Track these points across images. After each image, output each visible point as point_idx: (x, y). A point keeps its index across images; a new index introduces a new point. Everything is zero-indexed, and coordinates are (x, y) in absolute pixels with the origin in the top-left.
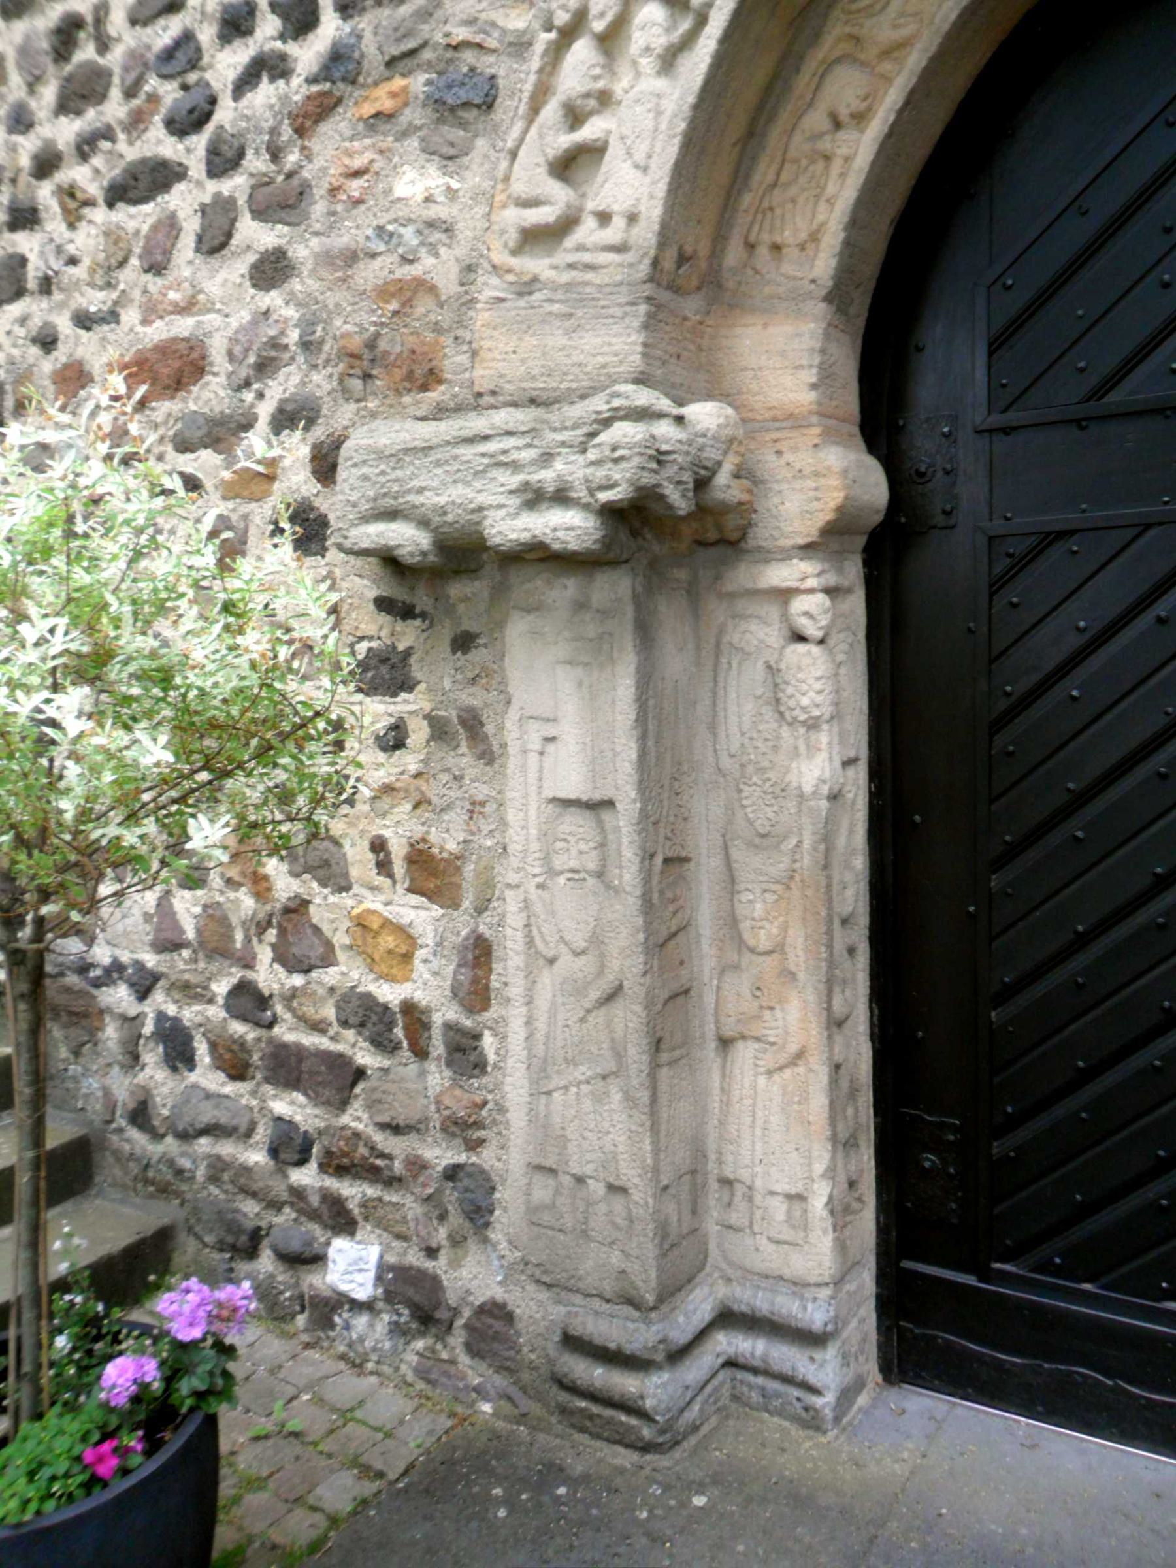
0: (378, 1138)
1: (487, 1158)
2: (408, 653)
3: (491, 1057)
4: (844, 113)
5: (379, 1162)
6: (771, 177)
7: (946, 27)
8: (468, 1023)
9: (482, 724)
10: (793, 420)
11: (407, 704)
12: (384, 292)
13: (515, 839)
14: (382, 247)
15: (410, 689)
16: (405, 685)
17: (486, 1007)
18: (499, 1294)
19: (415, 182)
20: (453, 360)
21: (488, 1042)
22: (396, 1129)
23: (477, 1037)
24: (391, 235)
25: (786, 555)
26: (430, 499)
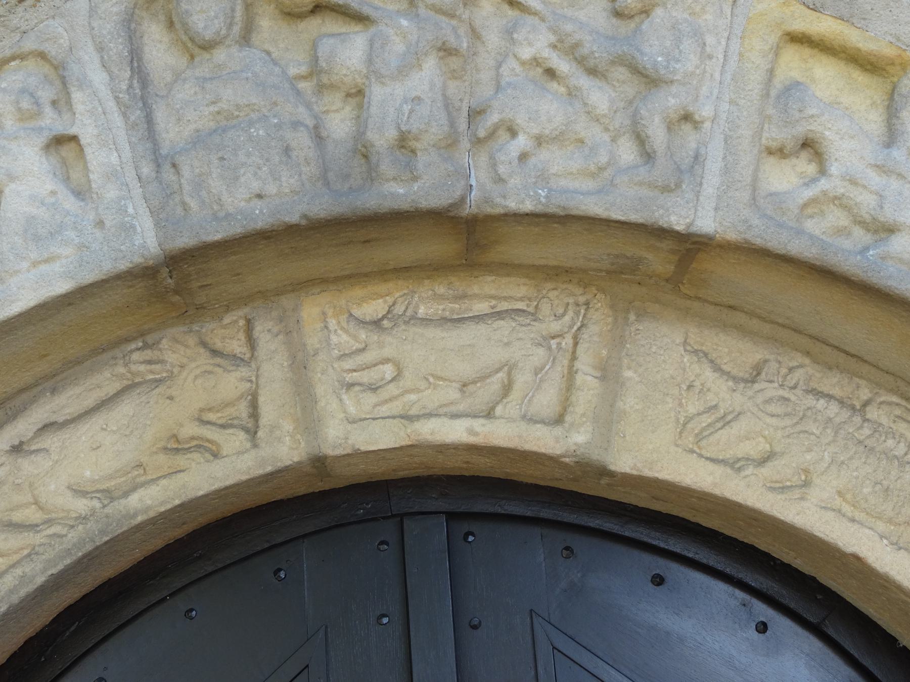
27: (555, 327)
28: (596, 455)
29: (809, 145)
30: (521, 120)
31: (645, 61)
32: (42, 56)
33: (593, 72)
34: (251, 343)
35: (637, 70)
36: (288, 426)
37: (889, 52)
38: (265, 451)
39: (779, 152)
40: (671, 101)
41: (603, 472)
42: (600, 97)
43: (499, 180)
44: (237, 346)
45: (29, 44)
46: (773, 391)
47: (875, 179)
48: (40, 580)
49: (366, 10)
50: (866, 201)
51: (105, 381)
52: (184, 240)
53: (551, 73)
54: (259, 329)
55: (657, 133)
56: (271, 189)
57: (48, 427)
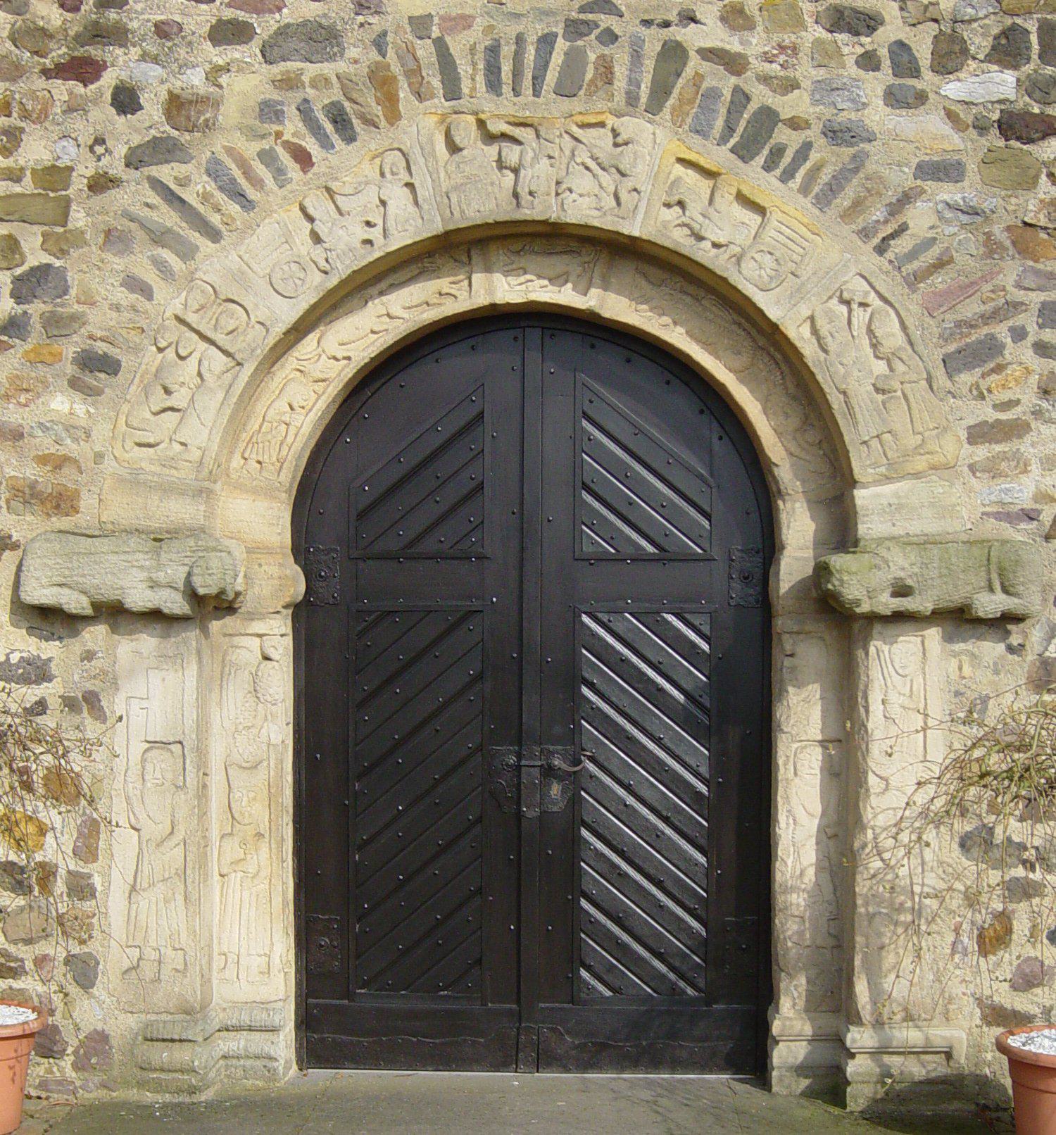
0: (12, 949)
1: (93, 947)
2: (50, 660)
3: (99, 888)
4: (295, 405)
5: (12, 964)
6: (256, 427)
7: (346, 380)
8: (85, 871)
9: (100, 701)
10: (269, 551)
11: (50, 691)
12: (43, 460)
13: (119, 764)
14: (40, 434)
15: (50, 681)
16: (49, 679)
17: (95, 858)
18: (99, 1028)
19: (61, 403)
20: (87, 502)
21: (97, 881)
22: (29, 942)
23: (90, 876)
24: (48, 429)
25: (262, 617)
26: (88, 582)
27: (587, 259)
28: (597, 310)
29: (681, 204)
30: (574, 188)
31: (621, 167)
32: (400, 150)
33: (603, 169)
34: (469, 257)
35: (619, 171)
36: (482, 292)
37: (714, 169)
38: (474, 300)
39: (668, 205)
40: (629, 183)
41: (599, 316)
42: (606, 179)
43: (564, 210)
44: (465, 259)
45: (396, 146)
46: (667, 290)
47: (700, 219)
48: (391, 342)
49: (520, 139)
50: (696, 226)
51: (414, 269)
52: (452, 227)
53: (587, 168)
54: (473, 252)
55: (624, 196)
56: (482, 209)
57: (392, 285)
